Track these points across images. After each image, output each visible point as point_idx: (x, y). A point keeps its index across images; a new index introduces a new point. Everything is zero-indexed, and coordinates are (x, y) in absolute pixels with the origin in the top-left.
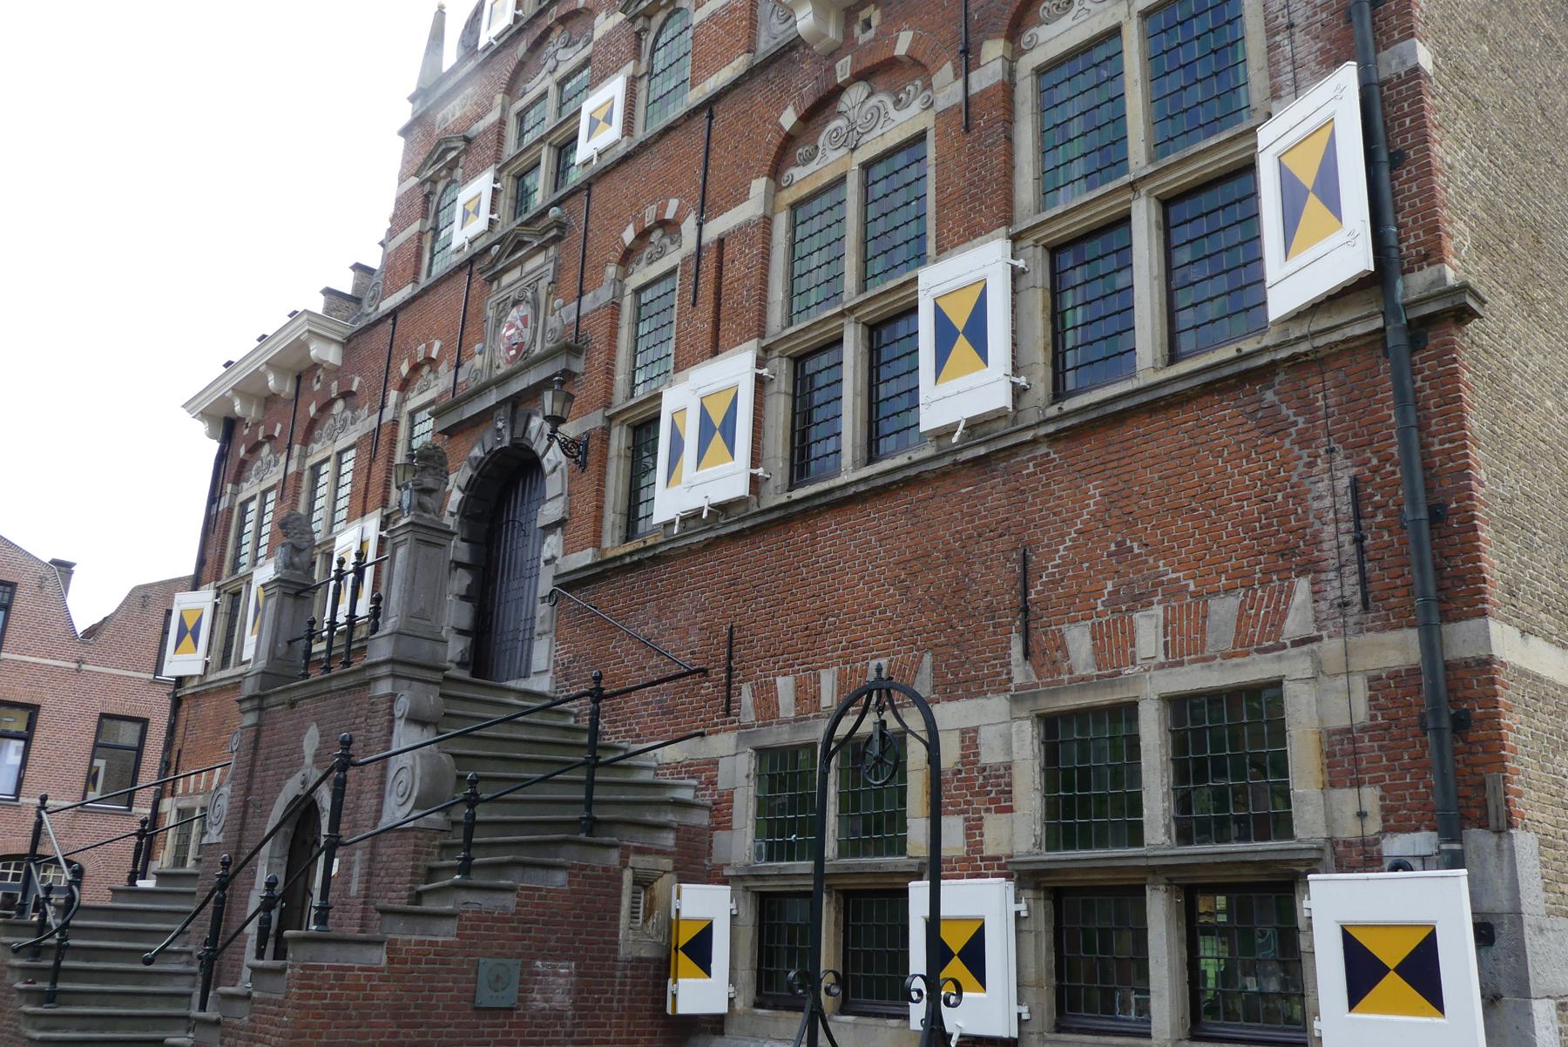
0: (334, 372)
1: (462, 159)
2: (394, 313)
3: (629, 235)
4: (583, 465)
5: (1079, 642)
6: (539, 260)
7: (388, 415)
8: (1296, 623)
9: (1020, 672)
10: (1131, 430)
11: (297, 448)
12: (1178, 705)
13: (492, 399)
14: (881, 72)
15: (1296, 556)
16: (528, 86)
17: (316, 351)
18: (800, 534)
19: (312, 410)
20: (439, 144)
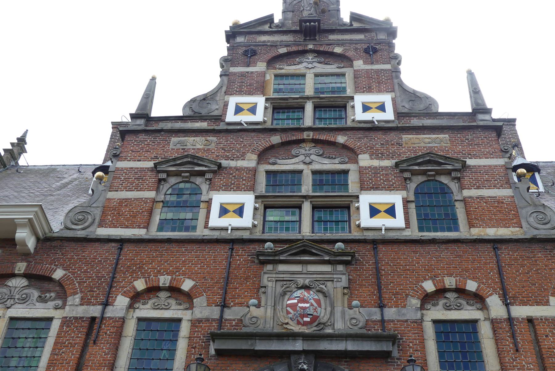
0: (26, 255)
1: (208, 176)
2: (122, 242)
3: (429, 286)
6: (327, 268)
7: (110, 312)
16: (279, 161)
17: (23, 235)
20: (187, 156)
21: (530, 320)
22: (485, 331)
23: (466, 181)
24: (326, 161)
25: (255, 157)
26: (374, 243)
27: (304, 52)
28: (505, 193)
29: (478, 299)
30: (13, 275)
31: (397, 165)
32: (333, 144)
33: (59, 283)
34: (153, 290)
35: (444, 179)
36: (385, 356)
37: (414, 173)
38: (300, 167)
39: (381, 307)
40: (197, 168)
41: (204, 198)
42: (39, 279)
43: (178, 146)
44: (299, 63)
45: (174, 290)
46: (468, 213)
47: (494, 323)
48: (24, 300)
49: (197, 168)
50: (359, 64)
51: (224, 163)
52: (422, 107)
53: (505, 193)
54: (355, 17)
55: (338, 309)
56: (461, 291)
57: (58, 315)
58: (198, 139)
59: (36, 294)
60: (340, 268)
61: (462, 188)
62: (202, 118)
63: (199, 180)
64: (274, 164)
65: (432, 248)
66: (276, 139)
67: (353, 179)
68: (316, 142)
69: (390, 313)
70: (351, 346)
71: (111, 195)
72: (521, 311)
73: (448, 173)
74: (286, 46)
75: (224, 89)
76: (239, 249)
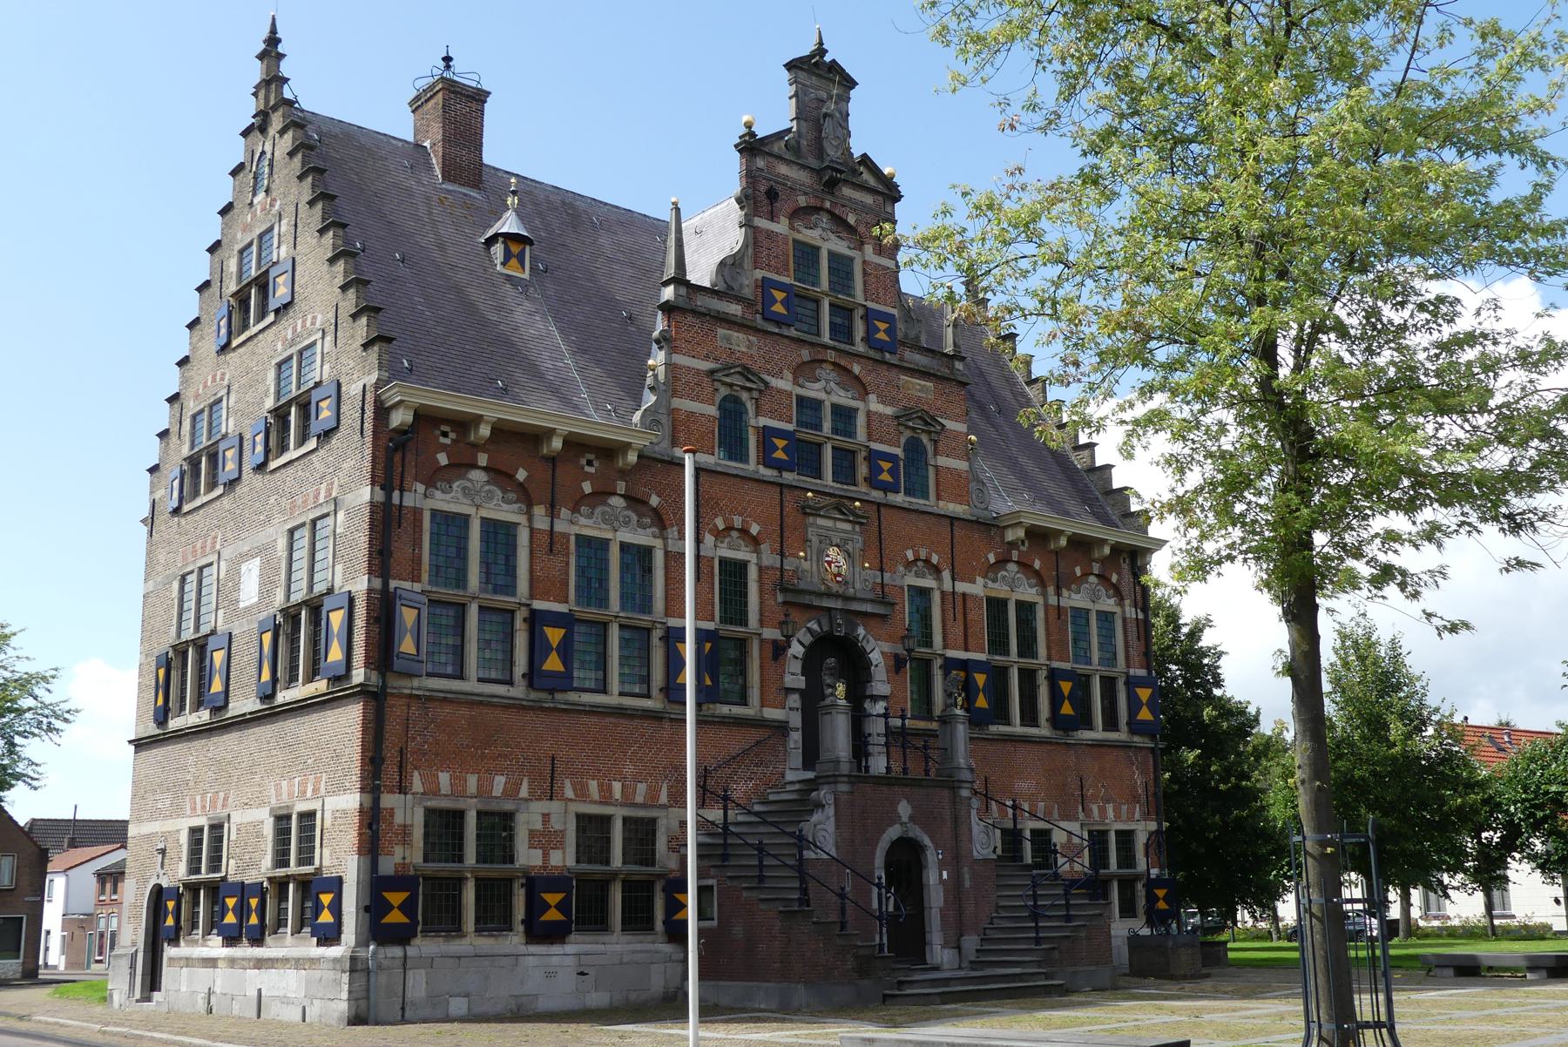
0: (624, 474)
1: (755, 394)
3: (910, 555)
4: (897, 672)
5: (1095, 808)
6: (848, 527)
8: (1137, 816)
9: (1081, 815)
10: (1104, 750)
11: (565, 513)
12: (1118, 832)
13: (838, 604)
14: (1025, 566)
15: (1135, 798)
18: (1009, 747)
19: (587, 488)
21: (964, 595)
22: (936, 598)
23: (941, 446)
24: (842, 393)
25: (790, 377)
26: (879, 505)
27: (818, 209)
28: (962, 465)
29: (936, 571)
30: (615, 494)
31: (897, 417)
32: (848, 371)
33: (655, 510)
34: (729, 528)
35: (925, 439)
36: (883, 617)
37: (908, 427)
38: (822, 396)
39: (882, 570)
40: (748, 385)
41: (753, 422)
42: (635, 501)
43: (725, 344)
44: (816, 226)
45: (744, 532)
46: (937, 484)
47: (943, 593)
48: (627, 523)
49: (748, 385)
50: (869, 249)
51: (768, 378)
52: (912, 334)
53: (962, 465)
54: (865, 159)
55: (857, 570)
56: (927, 561)
57: (658, 543)
58: (741, 336)
59: (635, 518)
60: (857, 528)
61: (936, 453)
62: (738, 299)
63: (745, 396)
64: (802, 387)
65: (913, 516)
66: (805, 354)
67: (861, 420)
68: (834, 364)
69: (887, 575)
70: (869, 608)
71: (677, 403)
72: (961, 587)
73: (930, 433)
74: (805, 194)
75: (750, 250)
76: (788, 496)
